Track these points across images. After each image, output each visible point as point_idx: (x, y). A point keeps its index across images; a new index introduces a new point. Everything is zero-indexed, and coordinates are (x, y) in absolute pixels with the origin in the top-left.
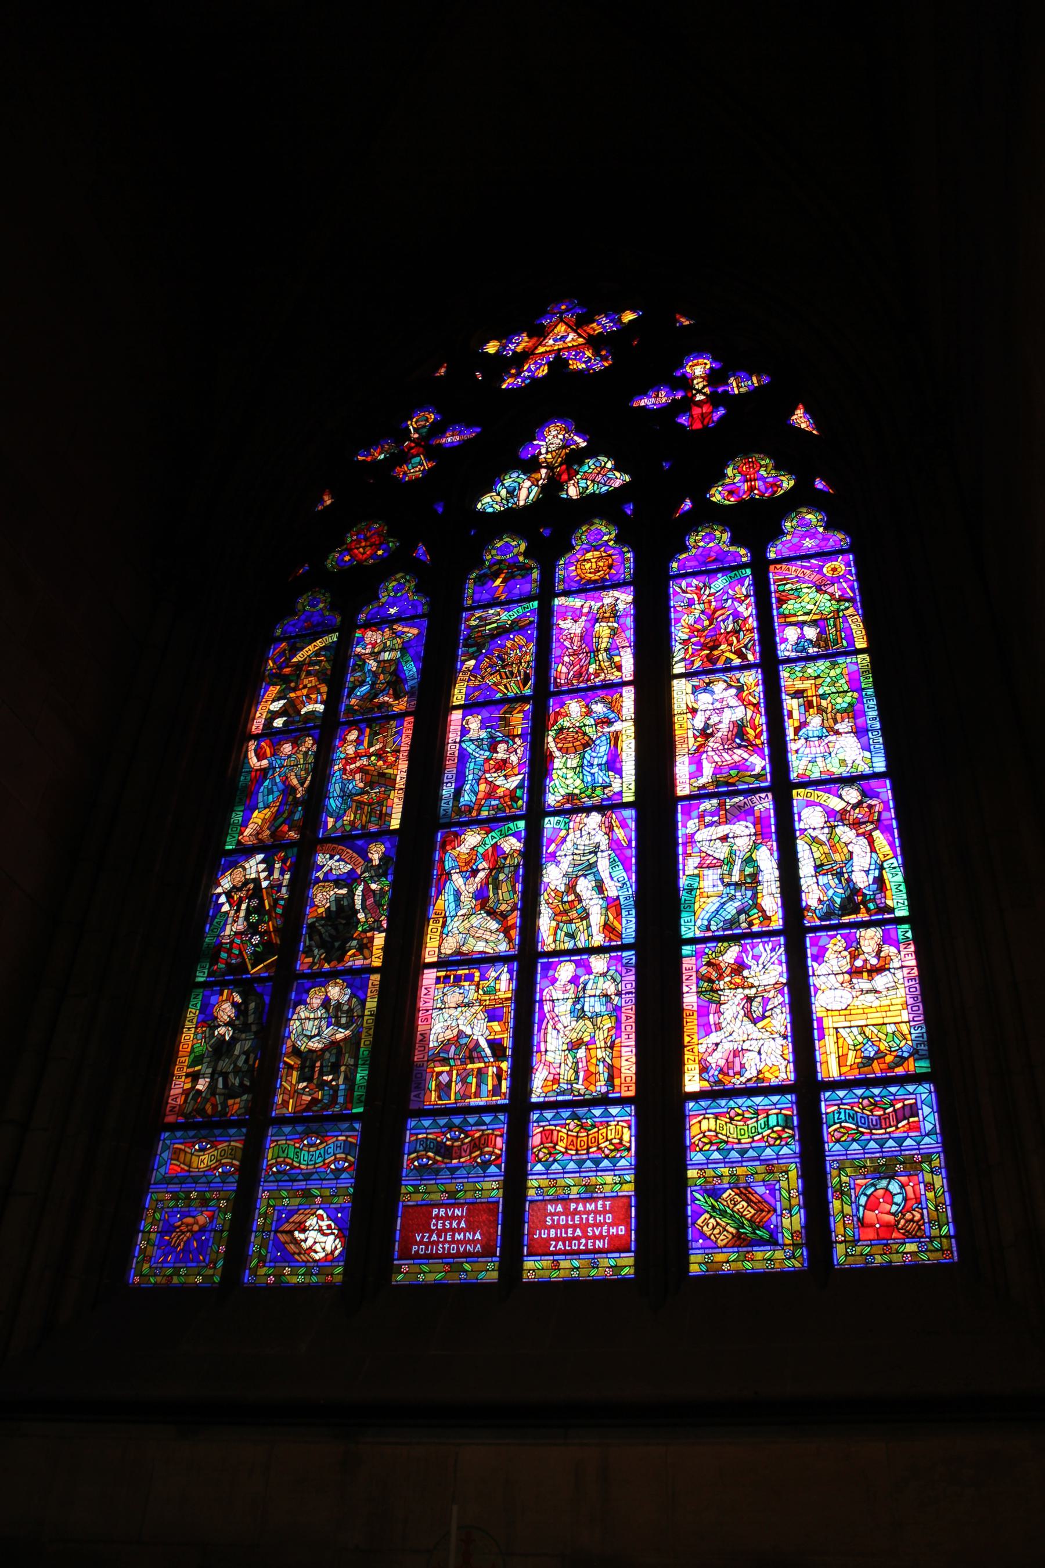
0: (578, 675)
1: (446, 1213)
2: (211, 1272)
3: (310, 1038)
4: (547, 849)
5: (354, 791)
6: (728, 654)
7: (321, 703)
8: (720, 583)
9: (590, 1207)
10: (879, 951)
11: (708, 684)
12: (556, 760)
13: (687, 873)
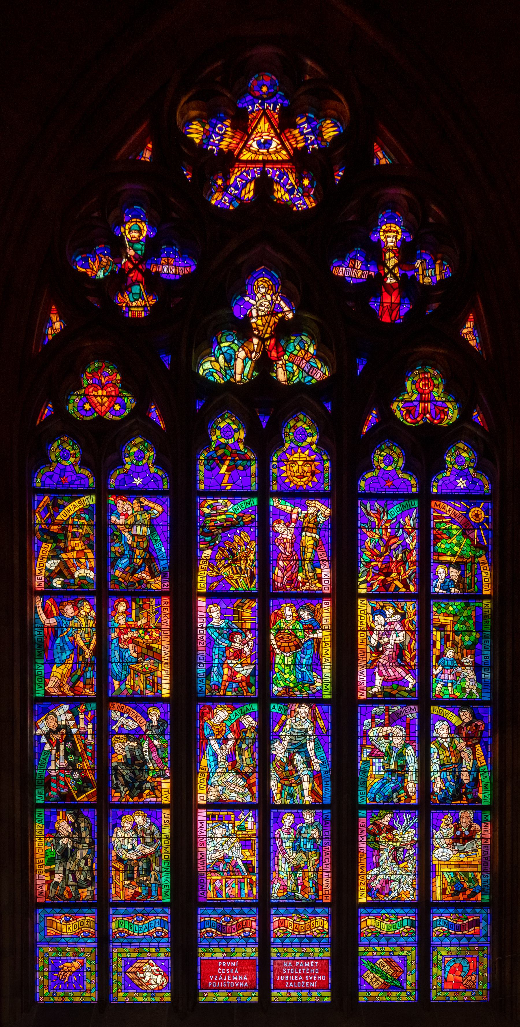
3: (128, 851)
6: (396, 582)
12: (277, 656)
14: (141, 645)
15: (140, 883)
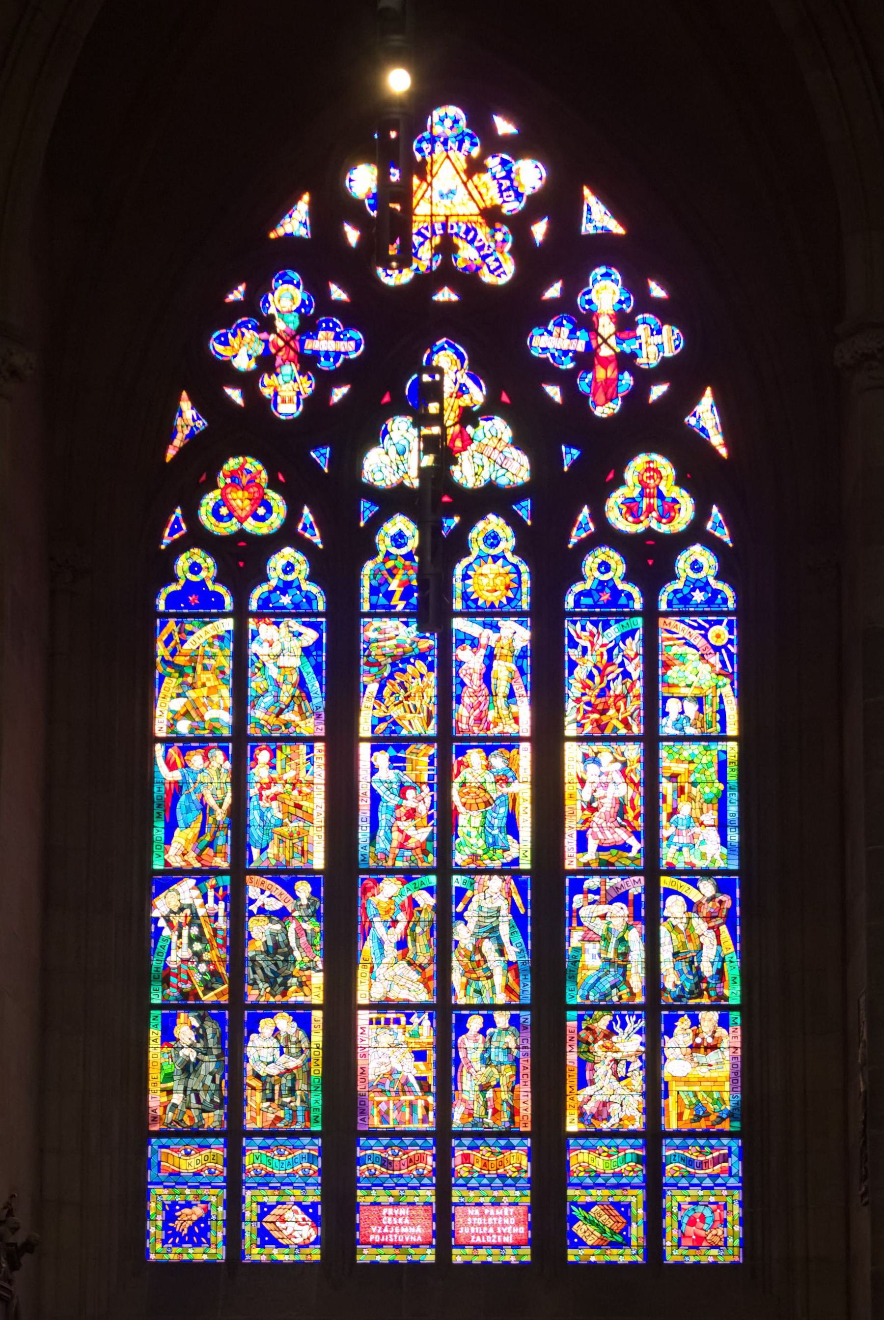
0: (479, 720)
2: (214, 1251)
10: (715, 1032)
11: (596, 754)
12: (460, 816)
13: (572, 945)
14: (287, 802)
15: (282, 1106)
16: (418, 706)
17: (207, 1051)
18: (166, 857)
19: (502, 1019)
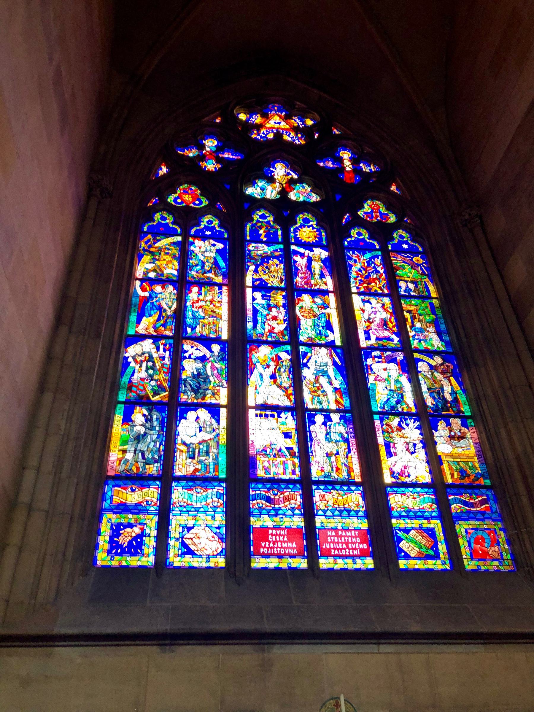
0: (306, 283)
1: (276, 533)
4: (303, 360)
5: (199, 317)
6: (375, 288)
7: (175, 270)
8: (368, 255)
9: (349, 534)
10: (460, 430)
15: (200, 462)
16: (276, 276)
17: (152, 428)
18: (137, 329)
19: (335, 417)
